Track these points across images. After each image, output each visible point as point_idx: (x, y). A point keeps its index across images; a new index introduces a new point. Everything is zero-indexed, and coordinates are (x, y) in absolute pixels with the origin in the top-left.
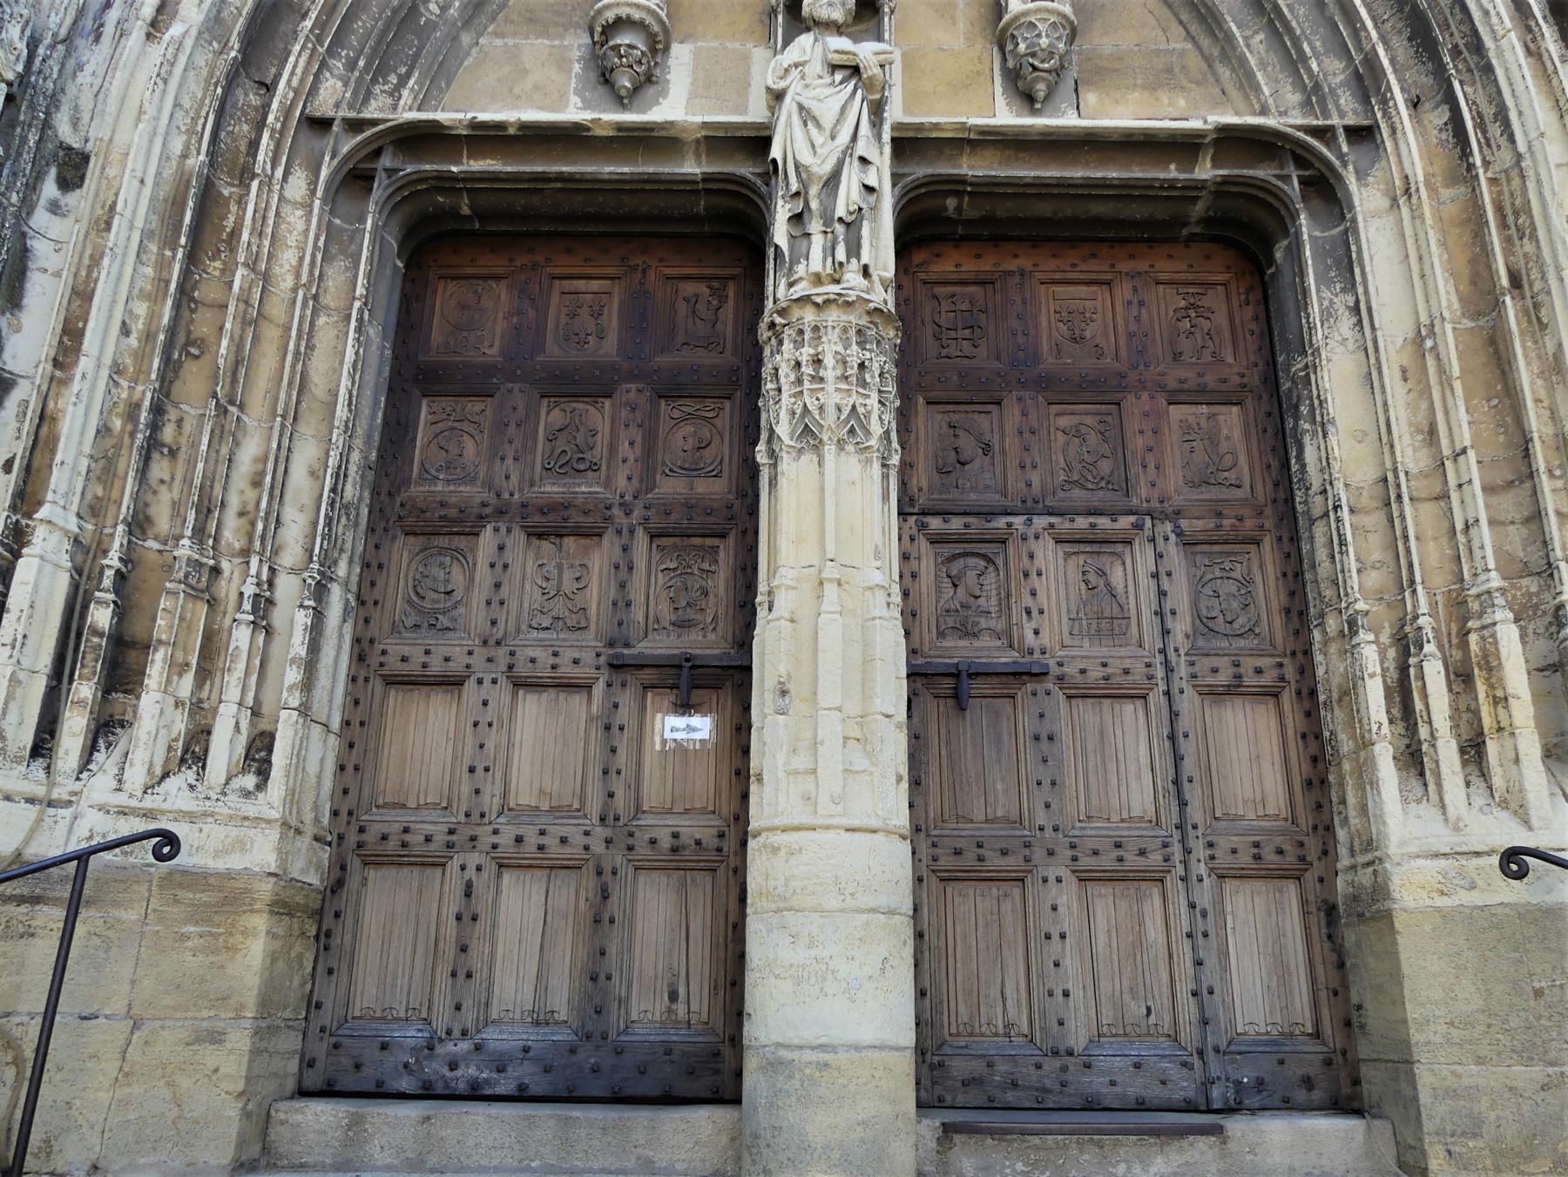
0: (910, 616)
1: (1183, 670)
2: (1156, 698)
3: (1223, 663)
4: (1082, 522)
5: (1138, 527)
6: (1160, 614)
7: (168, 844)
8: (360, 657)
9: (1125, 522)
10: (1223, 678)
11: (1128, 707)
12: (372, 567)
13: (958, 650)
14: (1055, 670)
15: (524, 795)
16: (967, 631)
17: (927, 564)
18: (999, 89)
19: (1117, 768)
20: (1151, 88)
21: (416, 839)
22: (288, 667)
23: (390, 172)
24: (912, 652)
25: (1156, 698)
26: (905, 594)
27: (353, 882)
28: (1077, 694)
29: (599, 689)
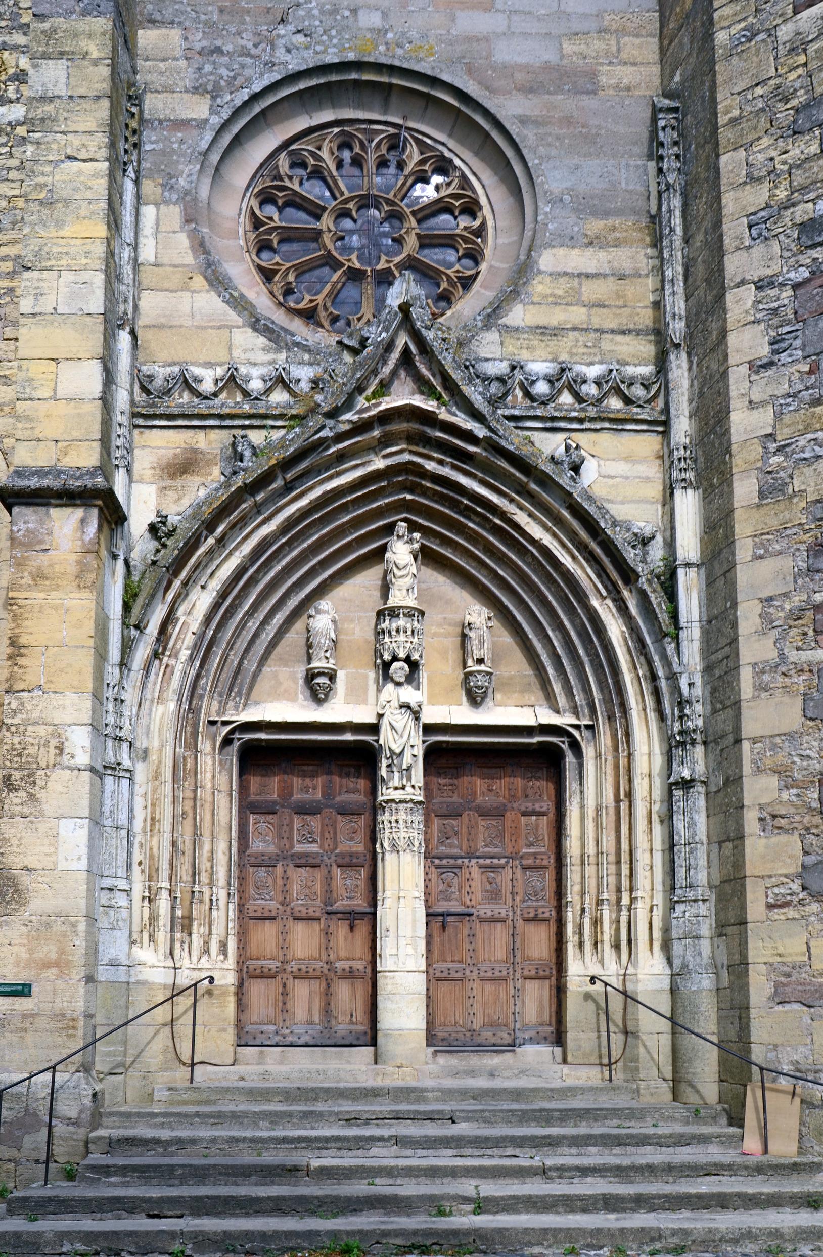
0: (427, 894)
1: (519, 912)
2: (509, 922)
3: (531, 910)
4: (488, 861)
5: (507, 862)
6: (512, 893)
7: (212, 980)
8: (240, 911)
9: (503, 861)
10: (532, 915)
11: (499, 925)
12: (242, 879)
13: (442, 906)
14: (476, 913)
15: (300, 954)
16: (448, 899)
17: (433, 876)
18: (464, 699)
19: (494, 946)
20: (522, 692)
21: (266, 970)
22: (223, 918)
23: (239, 739)
24: (427, 907)
25: (509, 922)
26: (426, 887)
27: (246, 984)
28: (482, 921)
29: (322, 920)
